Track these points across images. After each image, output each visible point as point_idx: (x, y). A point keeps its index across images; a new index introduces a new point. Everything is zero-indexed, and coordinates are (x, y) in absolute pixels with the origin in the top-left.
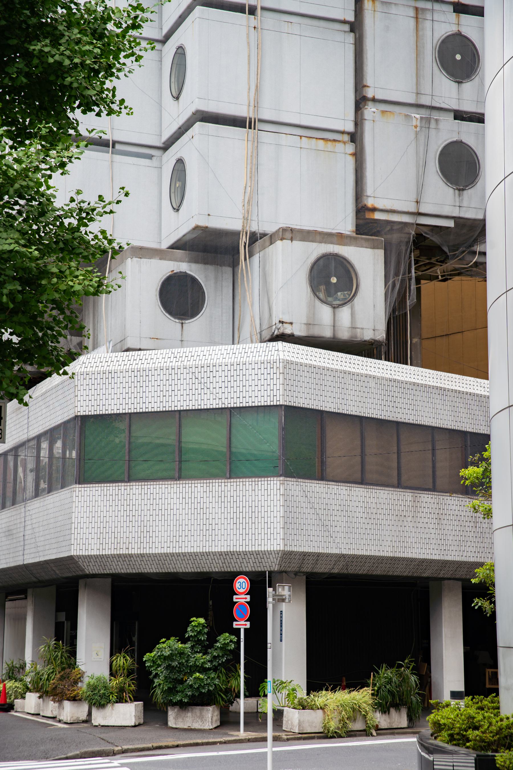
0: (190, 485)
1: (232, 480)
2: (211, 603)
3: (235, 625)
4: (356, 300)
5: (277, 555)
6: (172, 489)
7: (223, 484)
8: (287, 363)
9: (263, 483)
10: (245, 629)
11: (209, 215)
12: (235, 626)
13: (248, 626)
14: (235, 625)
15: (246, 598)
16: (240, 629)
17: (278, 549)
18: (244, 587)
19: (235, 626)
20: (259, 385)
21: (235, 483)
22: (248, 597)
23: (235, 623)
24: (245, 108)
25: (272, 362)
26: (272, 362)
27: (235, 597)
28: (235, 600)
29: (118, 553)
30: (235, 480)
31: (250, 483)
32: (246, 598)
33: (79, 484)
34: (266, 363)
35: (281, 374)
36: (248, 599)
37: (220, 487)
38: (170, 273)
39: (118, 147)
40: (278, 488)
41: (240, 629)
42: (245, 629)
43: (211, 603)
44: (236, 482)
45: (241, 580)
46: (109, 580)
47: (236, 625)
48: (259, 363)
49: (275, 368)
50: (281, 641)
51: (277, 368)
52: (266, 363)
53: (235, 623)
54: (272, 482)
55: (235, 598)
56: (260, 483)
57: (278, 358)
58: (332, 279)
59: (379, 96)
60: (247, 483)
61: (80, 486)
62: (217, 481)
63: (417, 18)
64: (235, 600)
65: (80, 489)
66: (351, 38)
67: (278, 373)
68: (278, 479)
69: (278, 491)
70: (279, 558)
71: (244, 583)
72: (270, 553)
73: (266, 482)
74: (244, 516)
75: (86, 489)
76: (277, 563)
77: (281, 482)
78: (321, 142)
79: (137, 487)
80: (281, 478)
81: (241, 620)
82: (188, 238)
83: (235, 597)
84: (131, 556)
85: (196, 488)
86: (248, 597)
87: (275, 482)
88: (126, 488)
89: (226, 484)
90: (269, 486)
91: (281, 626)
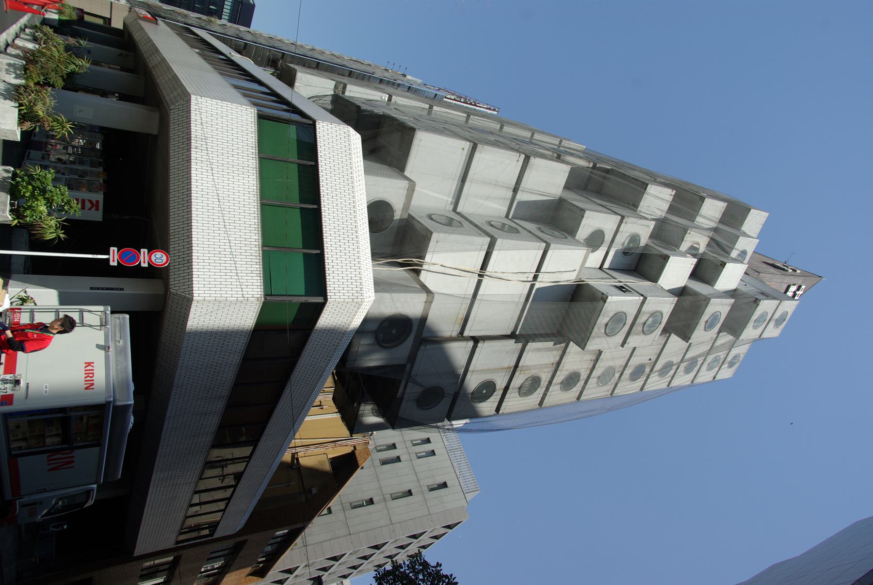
0: (256, 212)
1: (261, 252)
2: (127, 217)
3: (113, 250)
5: (187, 293)
6: (253, 196)
8: (359, 305)
9: (259, 281)
10: (108, 260)
11: (437, 242)
12: (112, 249)
13: (112, 263)
14: (113, 250)
15: (144, 262)
16: (108, 254)
17: (194, 295)
18: (157, 261)
19: (112, 249)
20: (343, 281)
21: (258, 255)
22: (146, 265)
23: (116, 249)
24: (490, 271)
25: (361, 292)
26: (361, 292)
27: (146, 251)
28: (142, 250)
29: (192, 138)
30: (261, 255)
31: (258, 269)
32: (144, 262)
33: (258, 113)
34: (361, 286)
35: (352, 300)
36: (143, 265)
37: (254, 240)
38: (394, 210)
40: (254, 296)
41: (108, 254)
42: (108, 260)
43: (127, 217)
44: (259, 256)
45: (164, 258)
46: (154, 131)
47: (114, 251)
48: (360, 281)
49: (357, 294)
50: (91, 288)
51: (357, 296)
52: (361, 286)
53: (116, 249)
54: (259, 290)
55: (144, 251)
56: (259, 278)
57: (365, 297)
58: (395, 330)
59: (478, 350)
60: (258, 266)
61: (256, 114)
62: (260, 238)
63: (508, 368)
64: (142, 250)
65: (253, 113)
66: (509, 333)
67: (353, 297)
68: (263, 296)
69: (251, 296)
70: (184, 294)
71: (161, 261)
73: (259, 284)
74: (227, 262)
75: (253, 118)
76: (178, 292)
77: (260, 299)
79: (255, 164)
80: (263, 299)
81: (120, 257)
82: (417, 226)
83: (146, 251)
84: (189, 150)
85: (253, 218)
86: (146, 265)
87: (259, 293)
88: (254, 154)
89: (257, 246)
90: (256, 287)
91: (107, 289)
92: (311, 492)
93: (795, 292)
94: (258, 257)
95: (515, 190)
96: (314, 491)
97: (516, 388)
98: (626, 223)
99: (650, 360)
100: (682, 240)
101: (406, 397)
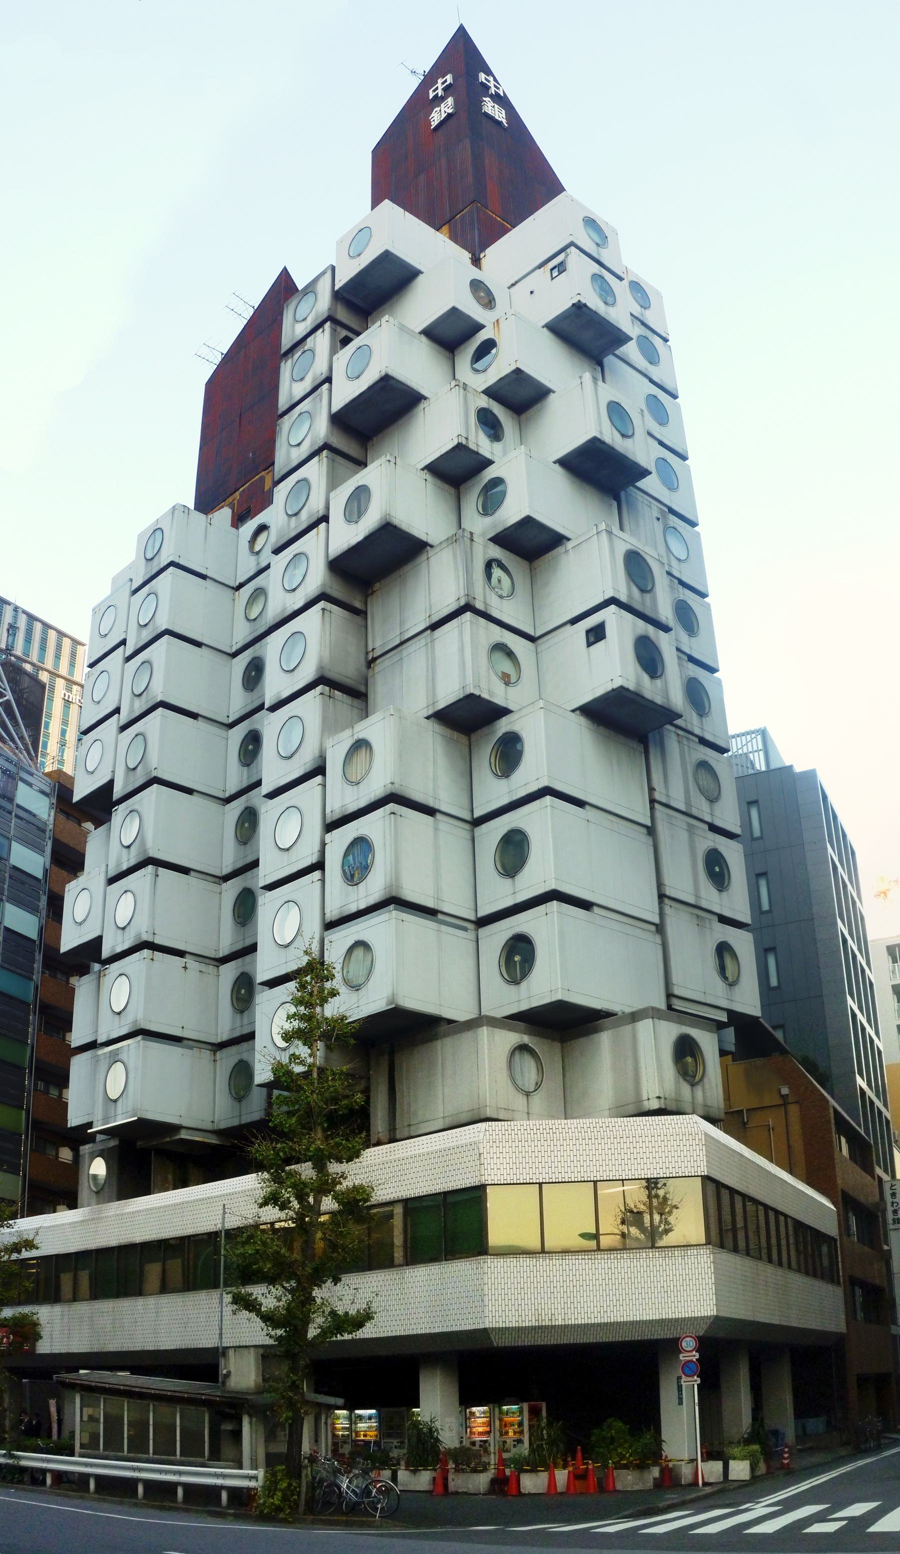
0: (615, 1255)
4: (706, 1080)
7: (651, 1254)
25: (693, 1134)
26: (693, 1134)
39: (440, 916)
50: (681, 1402)
59: (673, 895)
72: (702, 1318)
78: (639, 931)
80: (711, 1247)
92: (787, 1095)
93: (491, 96)
94: (667, 1253)
95: (430, 811)
96: (785, 1091)
97: (711, 809)
98: (474, 598)
99: (658, 519)
100: (477, 453)
101: (724, 1004)
